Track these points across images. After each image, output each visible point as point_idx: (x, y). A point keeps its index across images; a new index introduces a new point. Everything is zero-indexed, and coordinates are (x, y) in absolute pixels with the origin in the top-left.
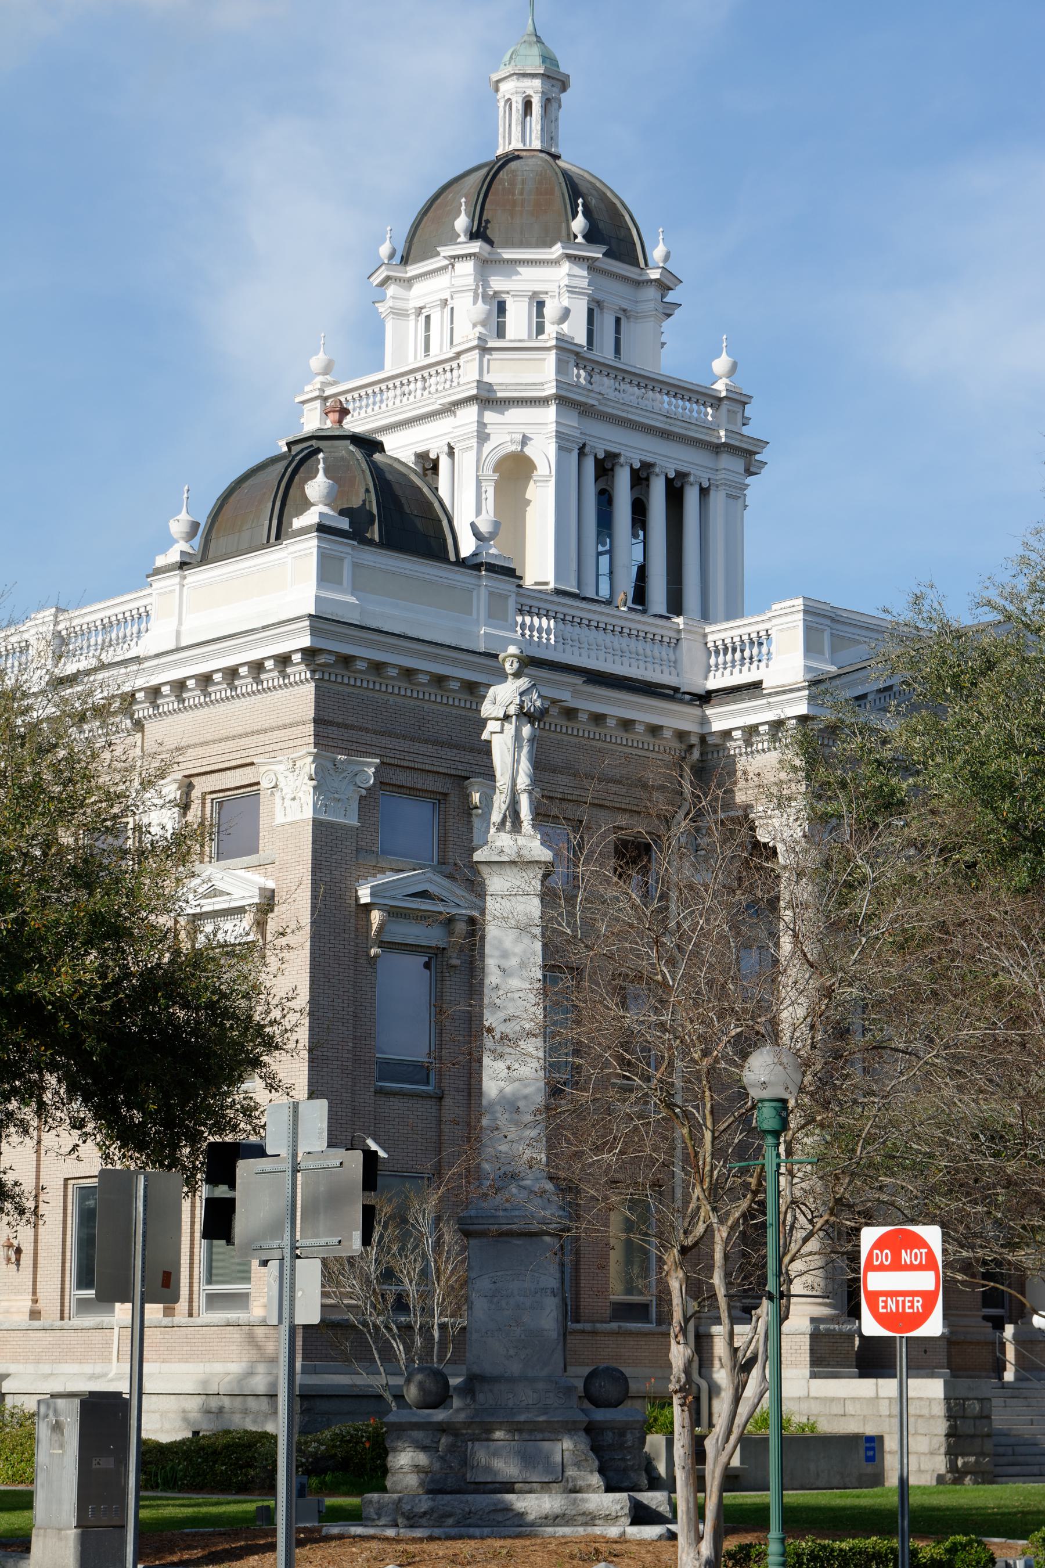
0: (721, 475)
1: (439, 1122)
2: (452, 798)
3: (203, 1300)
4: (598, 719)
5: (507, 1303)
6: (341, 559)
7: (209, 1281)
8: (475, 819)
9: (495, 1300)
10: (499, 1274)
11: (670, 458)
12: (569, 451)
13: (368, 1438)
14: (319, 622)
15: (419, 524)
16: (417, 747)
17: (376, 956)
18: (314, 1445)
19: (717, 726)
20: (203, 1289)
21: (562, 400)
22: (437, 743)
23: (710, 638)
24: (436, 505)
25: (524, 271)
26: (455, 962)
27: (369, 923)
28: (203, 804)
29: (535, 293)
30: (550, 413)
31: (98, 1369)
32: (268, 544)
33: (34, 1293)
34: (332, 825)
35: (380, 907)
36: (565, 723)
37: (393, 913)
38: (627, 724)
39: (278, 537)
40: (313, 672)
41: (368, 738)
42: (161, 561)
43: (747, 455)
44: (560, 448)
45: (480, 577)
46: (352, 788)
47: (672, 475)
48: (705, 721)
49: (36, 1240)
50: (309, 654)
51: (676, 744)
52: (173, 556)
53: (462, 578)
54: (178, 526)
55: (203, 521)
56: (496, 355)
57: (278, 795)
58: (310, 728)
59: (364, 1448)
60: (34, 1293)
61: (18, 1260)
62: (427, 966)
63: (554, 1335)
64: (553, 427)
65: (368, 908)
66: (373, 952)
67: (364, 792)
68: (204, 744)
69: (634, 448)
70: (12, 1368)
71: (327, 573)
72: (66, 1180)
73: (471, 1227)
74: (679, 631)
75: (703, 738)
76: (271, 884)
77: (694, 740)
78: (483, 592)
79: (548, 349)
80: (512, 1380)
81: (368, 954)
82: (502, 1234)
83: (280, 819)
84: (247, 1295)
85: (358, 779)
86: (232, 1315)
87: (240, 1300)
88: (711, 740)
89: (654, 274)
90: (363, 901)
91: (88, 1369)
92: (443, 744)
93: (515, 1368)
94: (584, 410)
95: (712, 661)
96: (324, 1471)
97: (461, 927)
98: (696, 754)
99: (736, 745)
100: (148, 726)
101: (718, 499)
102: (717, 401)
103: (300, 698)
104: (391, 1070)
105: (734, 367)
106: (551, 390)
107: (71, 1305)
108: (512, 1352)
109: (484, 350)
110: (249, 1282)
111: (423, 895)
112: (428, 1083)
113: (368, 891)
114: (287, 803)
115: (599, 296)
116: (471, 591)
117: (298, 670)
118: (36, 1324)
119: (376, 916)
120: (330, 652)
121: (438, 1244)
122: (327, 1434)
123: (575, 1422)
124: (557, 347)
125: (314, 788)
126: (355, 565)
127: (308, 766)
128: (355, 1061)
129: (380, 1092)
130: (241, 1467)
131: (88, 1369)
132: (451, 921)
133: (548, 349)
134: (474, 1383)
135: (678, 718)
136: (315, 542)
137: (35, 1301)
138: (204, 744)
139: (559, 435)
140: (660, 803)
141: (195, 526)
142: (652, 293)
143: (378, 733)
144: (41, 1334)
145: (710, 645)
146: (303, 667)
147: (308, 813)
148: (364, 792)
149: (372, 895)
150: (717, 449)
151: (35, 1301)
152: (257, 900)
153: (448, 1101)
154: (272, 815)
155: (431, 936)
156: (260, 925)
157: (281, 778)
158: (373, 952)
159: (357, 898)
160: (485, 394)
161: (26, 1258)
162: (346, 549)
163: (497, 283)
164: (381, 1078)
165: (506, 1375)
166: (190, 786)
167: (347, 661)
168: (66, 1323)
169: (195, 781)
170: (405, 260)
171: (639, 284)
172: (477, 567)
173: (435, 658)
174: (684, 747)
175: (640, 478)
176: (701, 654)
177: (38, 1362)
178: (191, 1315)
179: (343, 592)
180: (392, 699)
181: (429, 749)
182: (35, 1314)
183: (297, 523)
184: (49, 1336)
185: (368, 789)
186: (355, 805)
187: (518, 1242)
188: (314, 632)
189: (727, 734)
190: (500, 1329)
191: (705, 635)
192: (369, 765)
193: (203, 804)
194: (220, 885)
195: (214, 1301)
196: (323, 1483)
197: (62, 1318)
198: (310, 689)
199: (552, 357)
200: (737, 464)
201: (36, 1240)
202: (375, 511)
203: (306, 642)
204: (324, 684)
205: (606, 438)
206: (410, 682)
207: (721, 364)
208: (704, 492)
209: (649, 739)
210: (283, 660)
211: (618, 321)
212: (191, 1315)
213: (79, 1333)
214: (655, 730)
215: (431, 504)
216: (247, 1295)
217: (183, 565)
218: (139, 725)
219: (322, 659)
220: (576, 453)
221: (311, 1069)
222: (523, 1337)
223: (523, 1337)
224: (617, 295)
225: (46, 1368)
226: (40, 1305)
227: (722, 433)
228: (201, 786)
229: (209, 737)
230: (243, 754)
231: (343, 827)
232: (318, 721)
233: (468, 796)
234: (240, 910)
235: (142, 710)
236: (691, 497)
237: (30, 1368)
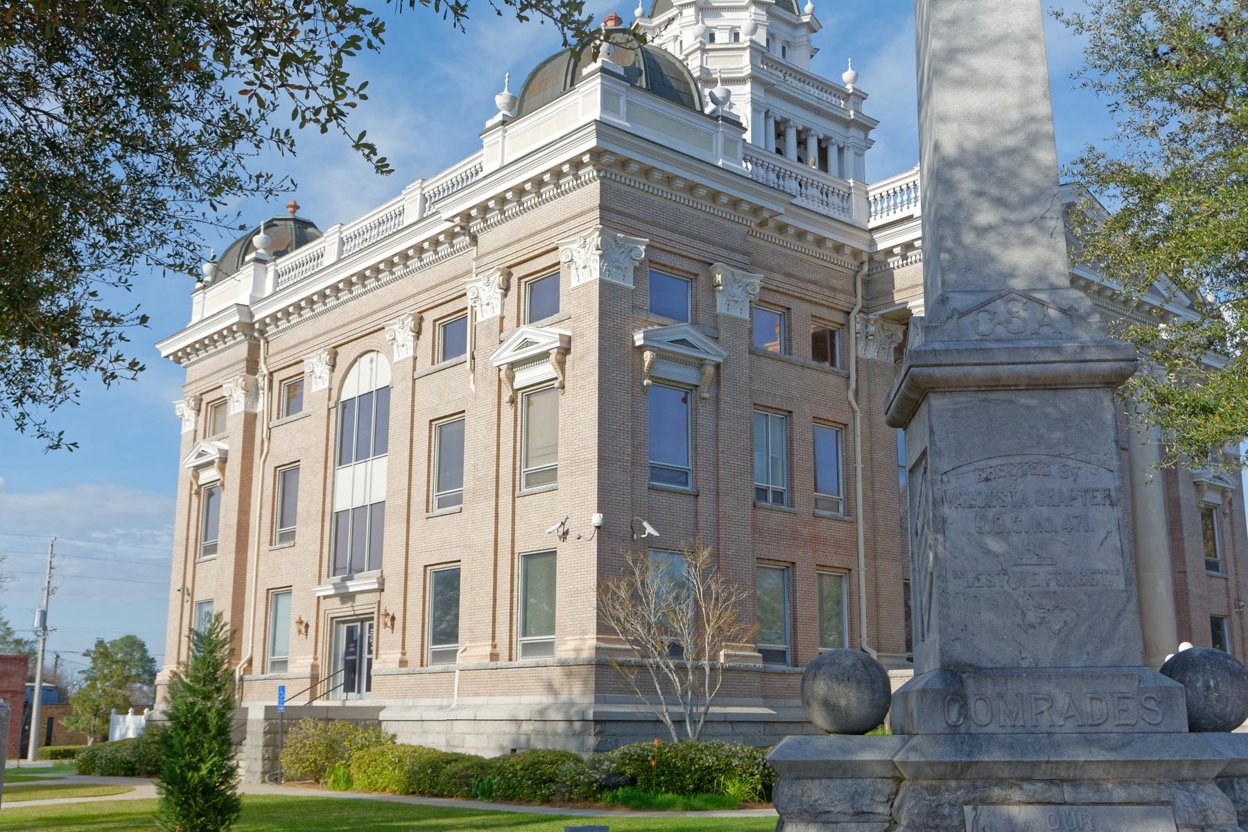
0: (851, 140)
1: (696, 514)
2: (701, 277)
3: (520, 648)
4: (801, 235)
5: (1016, 520)
6: (619, 96)
7: (524, 634)
8: (718, 295)
9: (991, 513)
10: (995, 462)
11: (821, 127)
12: (759, 112)
13: (653, 757)
14: (602, 127)
15: (673, 83)
16: (675, 237)
17: (648, 386)
18: (607, 763)
19: (881, 246)
20: (520, 640)
21: (755, 79)
22: (690, 236)
23: (871, 194)
24: (686, 74)
25: (726, 15)
26: (706, 395)
27: (642, 361)
28: (519, 286)
29: (733, 28)
30: (747, 87)
31: (445, 702)
32: (565, 91)
33: (403, 648)
34: (614, 285)
35: (652, 349)
36: (777, 235)
37: (661, 355)
38: (820, 241)
39: (572, 84)
40: (599, 171)
41: (640, 225)
42: (489, 124)
43: (865, 126)
44: (754, 110)
45: (717, 126)
46: (628, 260)
47: (821, 137)
48: (873, 243)
49: (405, 611)
50: (595, 153)
51: (851, 261)
52: (498, 118)
53: (707, 126)
54: (501, 100)
55: (518, 96)
56: (711, 54)
57: (573, 267)
58: (597, 213)
59: (650, 767)
60: (403, 648)
61: (393, 625)
62: (685, 400)
63: (1119, 583)
64: (749, 96)
65: (641, 349)
66: (645, 382)
67: (637, 264)
68: (519, 241)
69: (801, 119)
70: (387, 702)
71: (608, 102)
72: (426, 567)
73: (938, 372)
74: (850, 188)
75: (871, 260)
76: (569, 333)
77: (865, 258)
78: (720, 136)
79: (744, 49)
80: (1036, 673)
81: (642, 384)
82: (992, 386)
83: (574, 283)
84: (552, 643)
85: (633, 254)
86: (541, 659)
87: (548, 647)
88: (877, 258)
89: (806, 19)
90: (638, 344)
91: (438, 702)
92: (695, 237)
93: (1043, 650)
94: (769, 89)
95: (873, 209)
96: (616, 786)
97: (710, 370)
98: (866, 268)
99: (893, 262)
100: (480, 238)
101: (849, 155)
102: (846, 96)
103: (589, 194)
104: (658, 473)
105: (856, 76)
106: (747, 71)
107: (428, 656)
108: (1032, 617)
109: (704, 51)
110: (554, 633)
111: (682, 342)
112: (687, 484)
113: (642, 335)
114: (580, 271)
115: (772, 31)
116: (711, 135)
117: (588, 172)
118: (404, 670)
119: (648, 356)
120: (612, 153)
121: (707, 593)
122: (617, 753)
123: (1196, 763)
124: (750, 47)
125: (601, 256)
126: (629, 103)
127: (596, 239)
128: (633, 464)
129: (651, 488)
130: (545, 783)
131: (438, 702)
132: (701, 364)
133: (744, 49)
134: (955, 679)
135: (856, 242)
136: (599, 80)
137: (404, 654)
138: (519, 241)
139: (753, 102)
140: (842, 300)
141: (513, 99)
142: (804, 31)
143: (648, 223)
144: (406, 677)
145: (871, 199)
146: (591, 168)
147: (596, 275)
148: (637, 264)
149: (645, 338)
150: (848, 124)
151: (404, 654)
152: (558, 344)
153: (700, 498)
154: (569, 281)
155: (687, 375)
156: (561, 364)
157: (575, 254)
158: (645, 382)
159: (633, 342)
160: (705, 77)
161: (398, 624)
162: (621, 88)
163: (710, 22)
164: (652, 479)
165: (1024, 664)
166: (510, 275)
167: (624, 163)
168: (425, 669)
169: (513, 270)
170: (651, 17)
171: (796, 26)
172: (716, 119)
173: (689, 168)
174: (857, 263)
175: (802, 143)
176: (864, 205)
177: (404, 697)
178: (510, 660)
179: (621, 118)
180: (657, 200)
181: (684, 240)
182: (403, 663)
183: (585, 71)
184: (412, 679)
185: (641, 263)
186: (631, 273)
187: (1030, 400)
188: (600, 135)
189: (889, 252)
190: (1004, 572)
191: (867, 193)
192: (641, 243)
193: (519, 286)
194: (532, 338)
195: (528, 649)
196: (615, 798)
197: (422, 665)
198: (596, 185)
199: (747, 54)
200: (861, 135)
201: (405, 611)
202: (643, 68)
203: (592, 143)
204: (609, 182)
205: (782, 109)
206: (670, 187)
207: (847, 76)
208: (841, 150)
209: (834, 255)
210: (576, 164)
211: (784, 48)
212: (510, 660)
213: (433, 676)
214: (839, 248)
215: (682, 73)
216: (552, 643)
217: (504, 123)
218: (474, 240)
219: (606, 159)
220: (763, 115)
221: (600, 466)
222: (1053, 586)
223: (1053, 586)
224: (784, 32)
225: (409, 702)
226: (407, 657)
227: (852, 113)
228: (518, 272)
229: (522, 236)
230: (547, 242)
231: (622, 288)
232: (602, 207)
233: (713, 277)
234: (544, 356)
235: (475, 226)
236: (833, 153)
237: (399, 702)
